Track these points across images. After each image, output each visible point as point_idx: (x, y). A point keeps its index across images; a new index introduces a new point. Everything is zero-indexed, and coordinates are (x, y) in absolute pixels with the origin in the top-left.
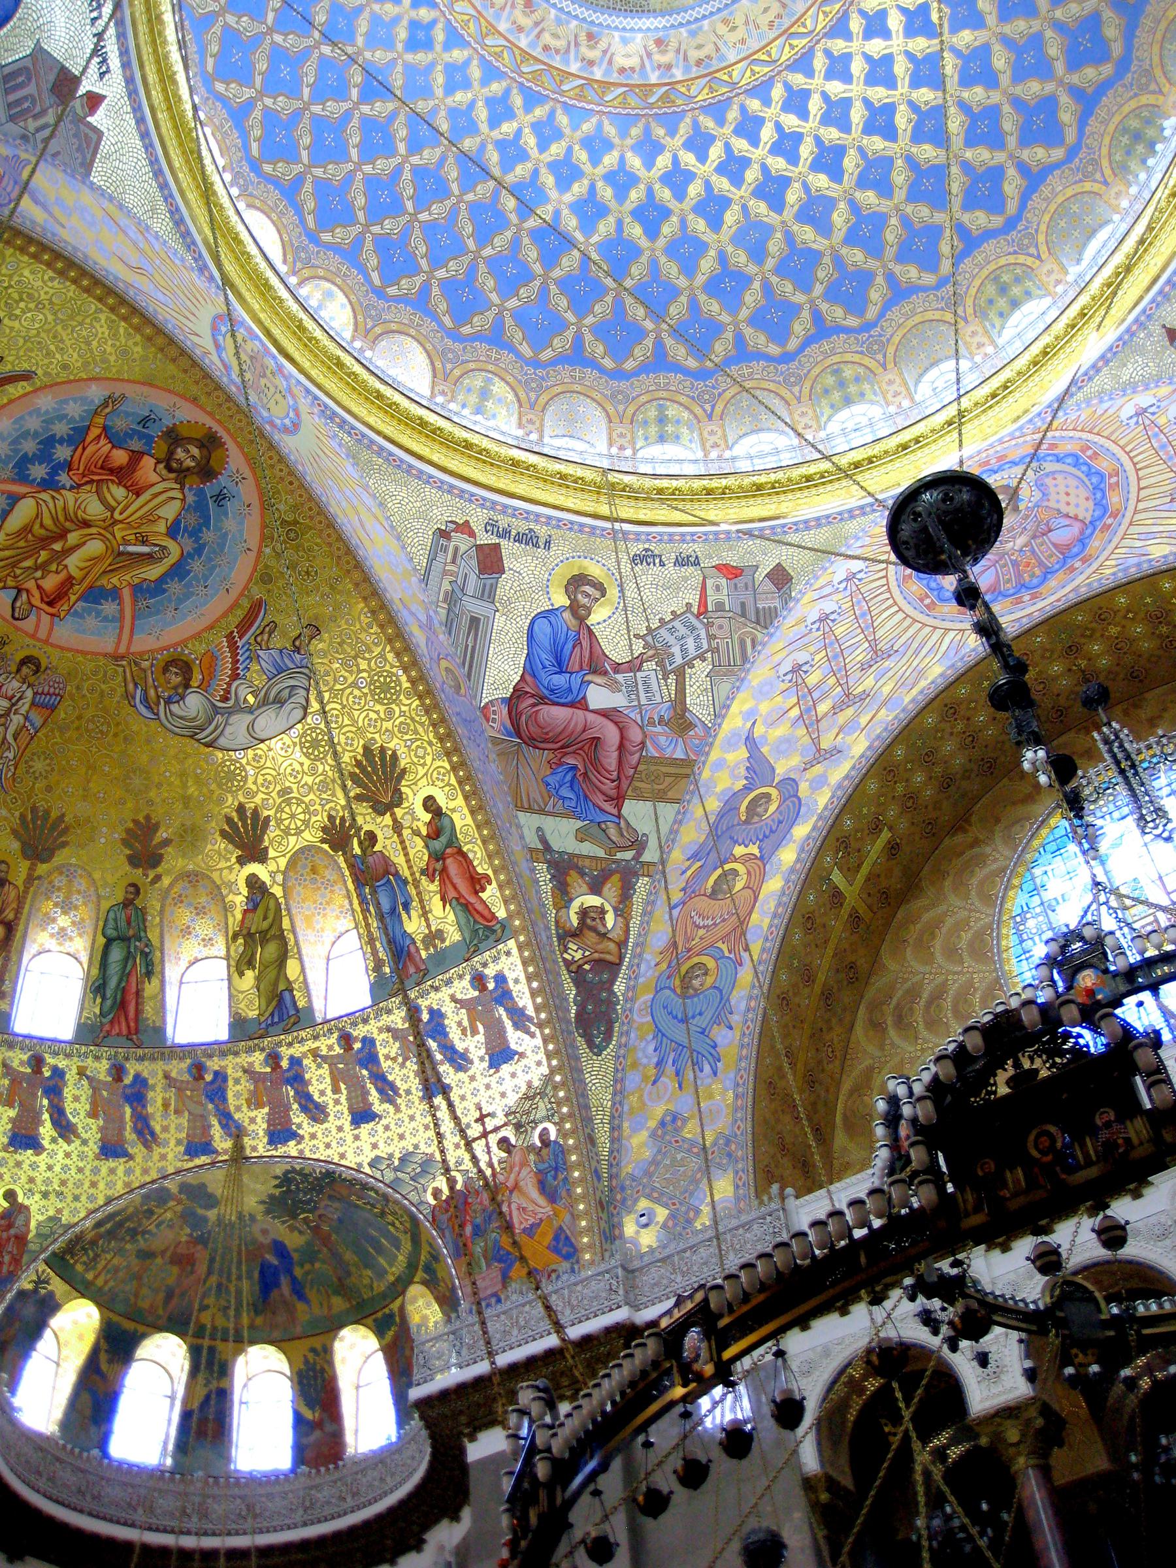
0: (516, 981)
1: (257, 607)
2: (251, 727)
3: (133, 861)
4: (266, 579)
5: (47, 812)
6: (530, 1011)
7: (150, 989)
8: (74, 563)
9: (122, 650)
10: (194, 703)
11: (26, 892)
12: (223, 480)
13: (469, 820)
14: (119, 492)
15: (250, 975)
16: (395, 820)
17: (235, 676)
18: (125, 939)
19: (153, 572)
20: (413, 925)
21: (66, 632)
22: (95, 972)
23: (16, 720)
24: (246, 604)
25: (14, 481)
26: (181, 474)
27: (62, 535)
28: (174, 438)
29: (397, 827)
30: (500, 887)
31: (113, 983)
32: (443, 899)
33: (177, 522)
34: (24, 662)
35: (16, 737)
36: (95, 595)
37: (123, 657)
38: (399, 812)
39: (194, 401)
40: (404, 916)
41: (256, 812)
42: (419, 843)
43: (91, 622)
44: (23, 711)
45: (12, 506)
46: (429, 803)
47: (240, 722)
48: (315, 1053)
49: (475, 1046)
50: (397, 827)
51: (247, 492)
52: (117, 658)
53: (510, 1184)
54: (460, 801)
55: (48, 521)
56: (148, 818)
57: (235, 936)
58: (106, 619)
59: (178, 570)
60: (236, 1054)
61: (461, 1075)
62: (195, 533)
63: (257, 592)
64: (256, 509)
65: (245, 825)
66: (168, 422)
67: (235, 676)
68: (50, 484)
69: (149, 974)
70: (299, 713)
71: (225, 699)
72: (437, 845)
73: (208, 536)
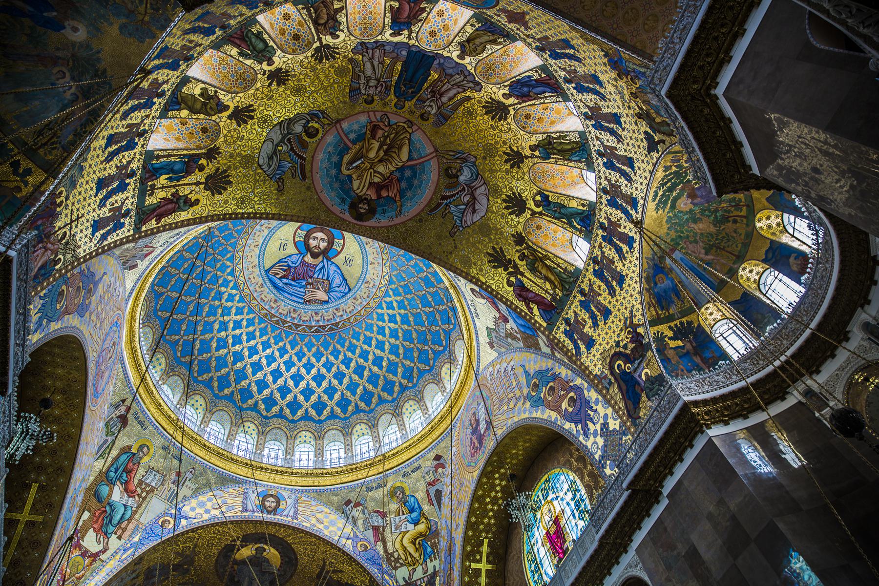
0: (118, 235)
1: (304, 177)
2: (272, 140)
3: (279, 70)
4: (308, 188)
5: (328, 59)
6: (106, 243)
7: (234, 51)
8: (376, 145)
9: (338, 125)
10: (298, 128)
11: (318, 36)
12: (346, 207)
13: (182, 219)
14: (376, 180)
15: (197, 91)
16: (201, 183)
17: (292, 149)
18: (261, 51)
19: (346, 159)
20: (163, 180)
21: (363, 119)
22: (265, 36)
23: (362, 81)
24: (308, 174)
25: (416, 165)
26: (361, 199)
27: (386, 152)
28: (372, 212)
29: (198, 184)
30: (153, 229)
31: (253, 40)
32: (163, 198)
33: (351, 182)
34: (372, 101)
35: (359, 76)
36: (361, 138)
37: (336, 123)
38: (202, 186)
39: (374, 228)
40: (168, 176)
41: (246, 123)
42: (187, 192)
43: (356, 127)
44: (362, 86)
45: (409, 155)
46: (197, 201)
47: (277, 138)
48: (147, 116)
49: (105, 212)
50: (198, 184)
51: (337, 209)
52: (339, 121)
53: (49, 246)
54: (190, 217)
55: (394, 155)
56: (285, 84)
57: (216, 92)
58: (351, 131)
59: (338, 165)
60: (177, 77)
61: (98, 201)
62: (342, 183)
63: (308, 182)
64: (329, 206)
65: (246, 116)
66: (377, 216)
67: (292, 149)
68: (401, 169)
69: (241, 54)
70: (261, 162)
71: (289, 140)
72: (182, 201)
73: (336, 185)
